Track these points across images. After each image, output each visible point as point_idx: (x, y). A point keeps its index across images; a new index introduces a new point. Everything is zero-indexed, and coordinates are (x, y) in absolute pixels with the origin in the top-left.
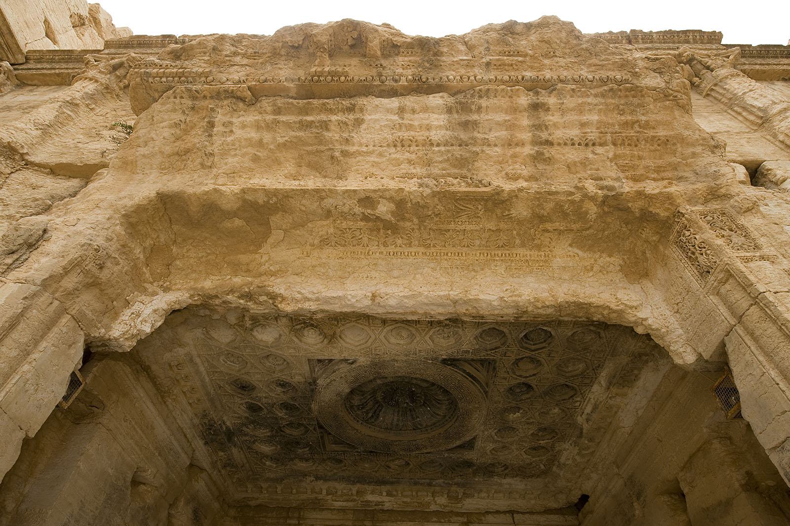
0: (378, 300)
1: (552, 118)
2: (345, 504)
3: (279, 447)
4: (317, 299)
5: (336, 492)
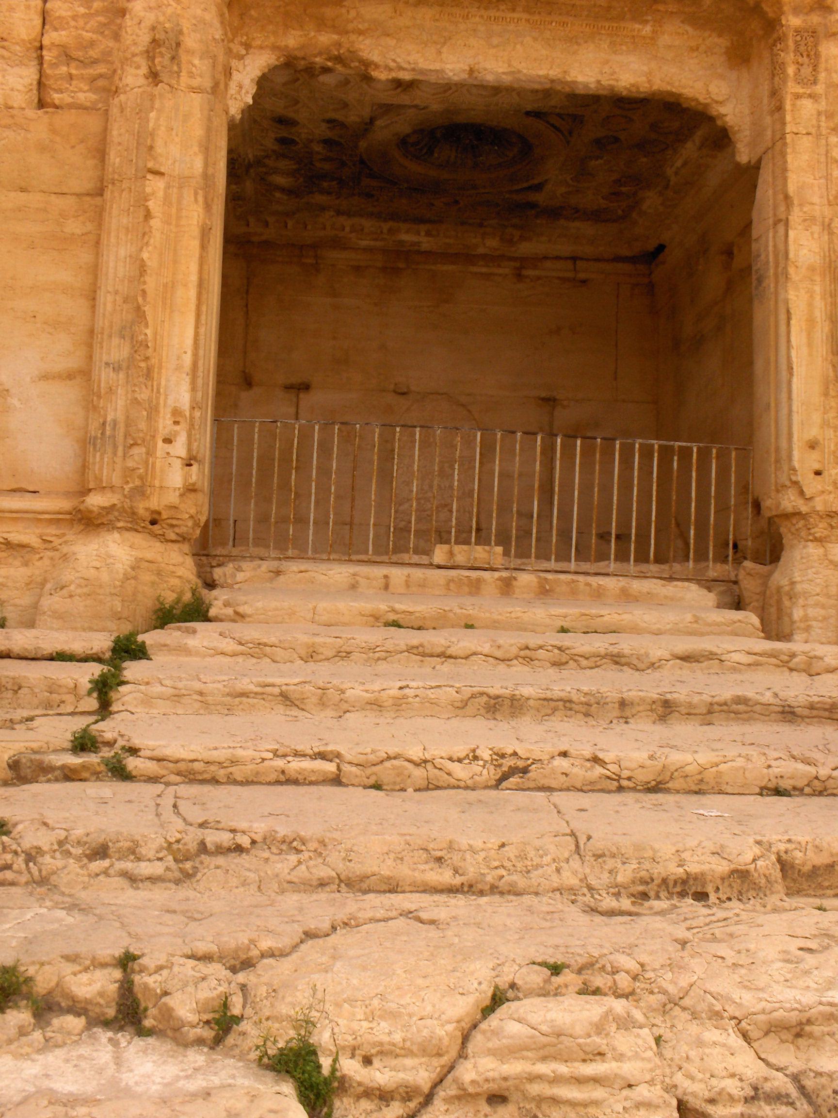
0: (476, 74)
2: (372, 243)
3: (302, 179)
4: (413, 70)
5: (362, 230)
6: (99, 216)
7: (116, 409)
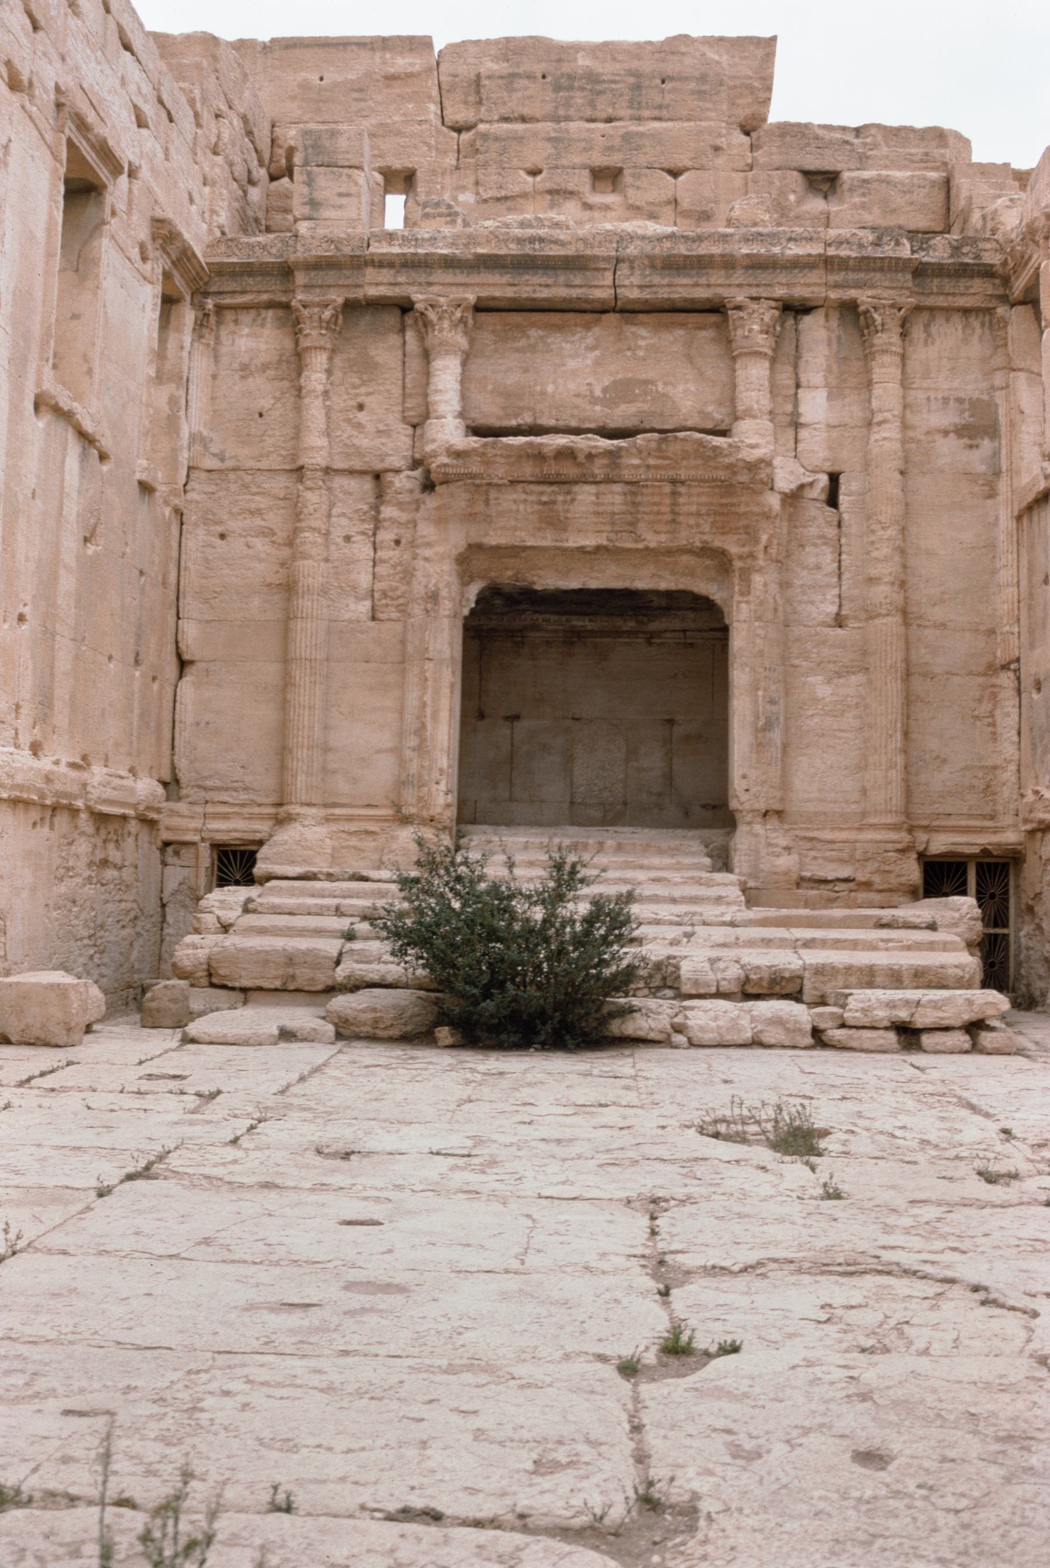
1: (681, 500)
6: (403, 673)
7: (413, 768)
